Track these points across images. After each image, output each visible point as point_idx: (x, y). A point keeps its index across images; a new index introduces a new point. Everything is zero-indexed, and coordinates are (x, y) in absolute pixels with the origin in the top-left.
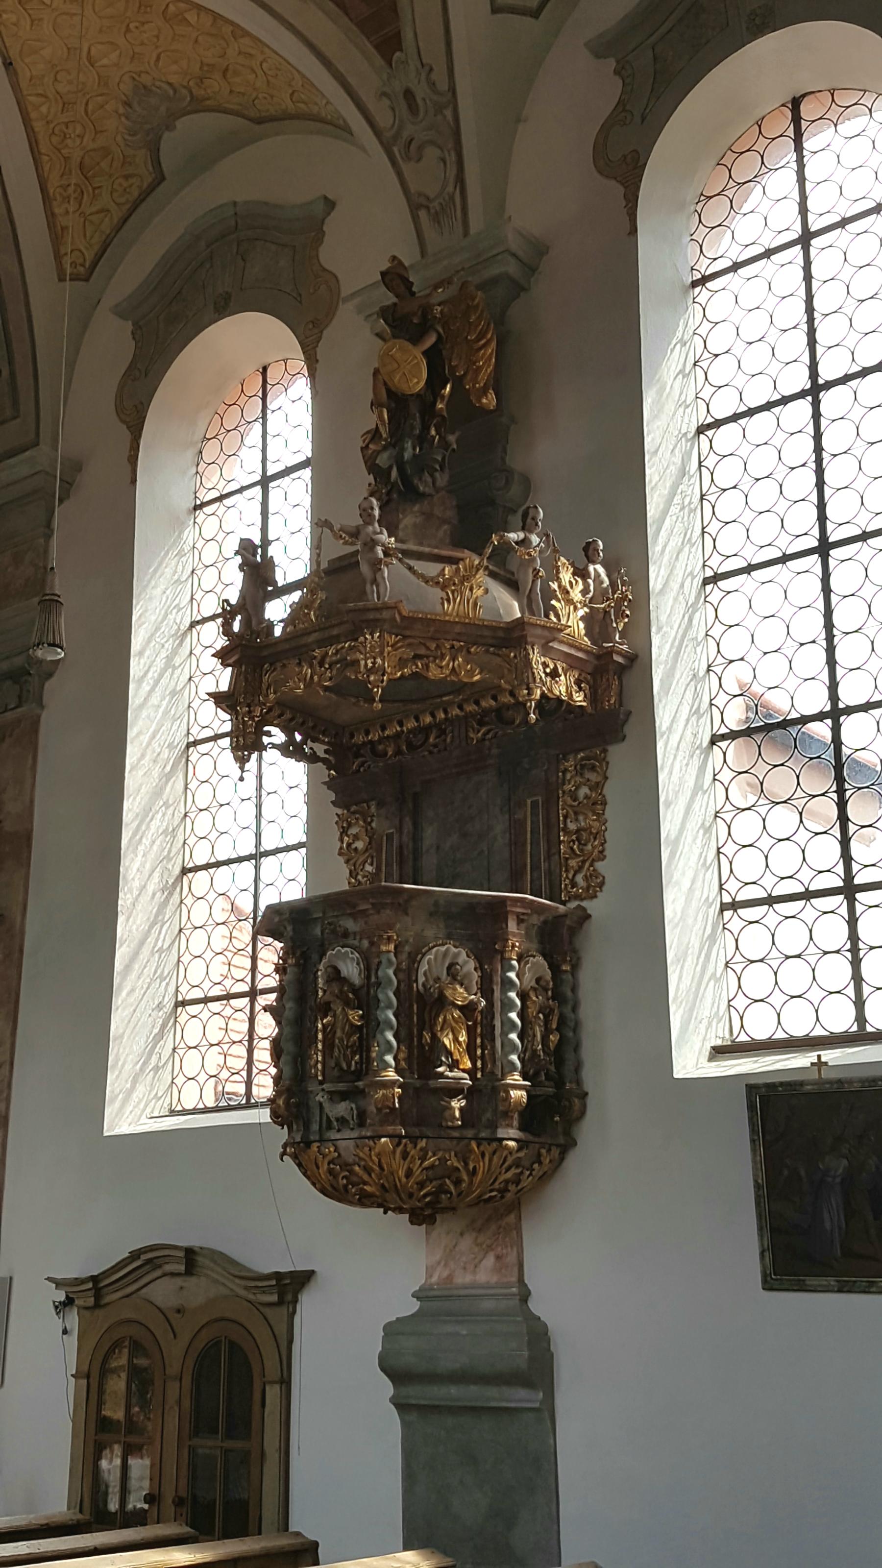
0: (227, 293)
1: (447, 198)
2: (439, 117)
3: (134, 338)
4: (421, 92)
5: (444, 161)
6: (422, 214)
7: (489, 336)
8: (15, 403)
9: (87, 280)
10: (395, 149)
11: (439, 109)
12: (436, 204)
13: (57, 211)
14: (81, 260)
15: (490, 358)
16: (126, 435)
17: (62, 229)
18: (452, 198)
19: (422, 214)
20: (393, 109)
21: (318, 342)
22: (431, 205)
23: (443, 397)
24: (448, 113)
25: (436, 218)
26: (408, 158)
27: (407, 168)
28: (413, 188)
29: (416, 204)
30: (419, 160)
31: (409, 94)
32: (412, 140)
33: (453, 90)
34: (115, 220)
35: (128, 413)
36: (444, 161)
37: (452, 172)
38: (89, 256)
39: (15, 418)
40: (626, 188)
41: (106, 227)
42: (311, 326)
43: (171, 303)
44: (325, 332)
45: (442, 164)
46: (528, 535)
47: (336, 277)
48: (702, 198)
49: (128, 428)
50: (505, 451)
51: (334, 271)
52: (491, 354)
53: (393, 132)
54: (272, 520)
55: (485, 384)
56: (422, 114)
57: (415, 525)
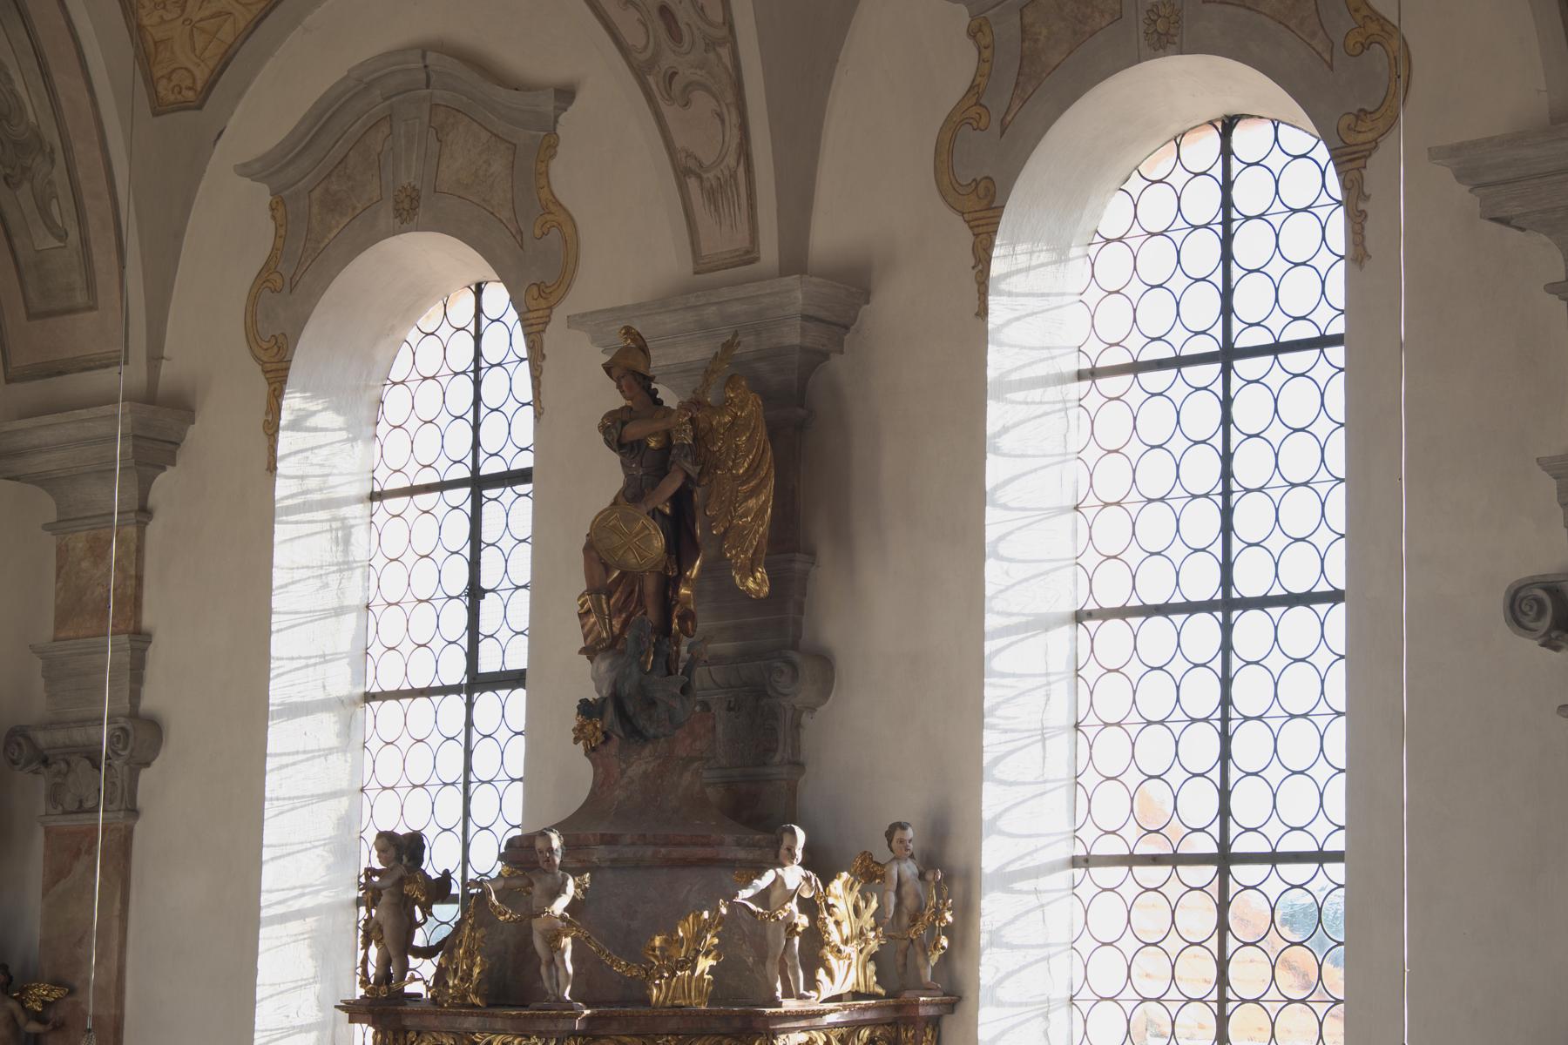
0: (414, 188)
1: (727, 172)
2: (712, 55)
3: (274, 217)
4: (684, 14)
6: (693, 183)
7: (763, 474)
8: (90, 286)
9: (200, 107)
10: (651, 79)
11: (712, 45)
12: (711, 175)
13: (146, 21)
14: (188, 82)
15: (762, 510)
16: (262, 386)
17: (155, 43)
18: (734, 176)
19: (693, 183)
20: (645, 25)
21: (547, 323)
22: (705, 176)
23: (687, 580)
24: (725, 52)
25: (712, 195)
27: (669, 111)
28: (680, 142)
30: (686, 104)
31: (665, 11)
32: (675, 74)
33: (729, 24)
34: (242, 25)
35: (265, 346)
38: (201, 74)
39: (91, 309)
40: (976, 235)
41: (227, 33)
42: (535, 289)
43: (329, 175)
44: (555, 310)
45: (717, 121)
46: (779, 870)
47: (572, 219)
48: (1097, 238)
49: (265, 372)
50: (801, 610)
51: (574, 215)
54: (487, 556)
56: (687, 38)
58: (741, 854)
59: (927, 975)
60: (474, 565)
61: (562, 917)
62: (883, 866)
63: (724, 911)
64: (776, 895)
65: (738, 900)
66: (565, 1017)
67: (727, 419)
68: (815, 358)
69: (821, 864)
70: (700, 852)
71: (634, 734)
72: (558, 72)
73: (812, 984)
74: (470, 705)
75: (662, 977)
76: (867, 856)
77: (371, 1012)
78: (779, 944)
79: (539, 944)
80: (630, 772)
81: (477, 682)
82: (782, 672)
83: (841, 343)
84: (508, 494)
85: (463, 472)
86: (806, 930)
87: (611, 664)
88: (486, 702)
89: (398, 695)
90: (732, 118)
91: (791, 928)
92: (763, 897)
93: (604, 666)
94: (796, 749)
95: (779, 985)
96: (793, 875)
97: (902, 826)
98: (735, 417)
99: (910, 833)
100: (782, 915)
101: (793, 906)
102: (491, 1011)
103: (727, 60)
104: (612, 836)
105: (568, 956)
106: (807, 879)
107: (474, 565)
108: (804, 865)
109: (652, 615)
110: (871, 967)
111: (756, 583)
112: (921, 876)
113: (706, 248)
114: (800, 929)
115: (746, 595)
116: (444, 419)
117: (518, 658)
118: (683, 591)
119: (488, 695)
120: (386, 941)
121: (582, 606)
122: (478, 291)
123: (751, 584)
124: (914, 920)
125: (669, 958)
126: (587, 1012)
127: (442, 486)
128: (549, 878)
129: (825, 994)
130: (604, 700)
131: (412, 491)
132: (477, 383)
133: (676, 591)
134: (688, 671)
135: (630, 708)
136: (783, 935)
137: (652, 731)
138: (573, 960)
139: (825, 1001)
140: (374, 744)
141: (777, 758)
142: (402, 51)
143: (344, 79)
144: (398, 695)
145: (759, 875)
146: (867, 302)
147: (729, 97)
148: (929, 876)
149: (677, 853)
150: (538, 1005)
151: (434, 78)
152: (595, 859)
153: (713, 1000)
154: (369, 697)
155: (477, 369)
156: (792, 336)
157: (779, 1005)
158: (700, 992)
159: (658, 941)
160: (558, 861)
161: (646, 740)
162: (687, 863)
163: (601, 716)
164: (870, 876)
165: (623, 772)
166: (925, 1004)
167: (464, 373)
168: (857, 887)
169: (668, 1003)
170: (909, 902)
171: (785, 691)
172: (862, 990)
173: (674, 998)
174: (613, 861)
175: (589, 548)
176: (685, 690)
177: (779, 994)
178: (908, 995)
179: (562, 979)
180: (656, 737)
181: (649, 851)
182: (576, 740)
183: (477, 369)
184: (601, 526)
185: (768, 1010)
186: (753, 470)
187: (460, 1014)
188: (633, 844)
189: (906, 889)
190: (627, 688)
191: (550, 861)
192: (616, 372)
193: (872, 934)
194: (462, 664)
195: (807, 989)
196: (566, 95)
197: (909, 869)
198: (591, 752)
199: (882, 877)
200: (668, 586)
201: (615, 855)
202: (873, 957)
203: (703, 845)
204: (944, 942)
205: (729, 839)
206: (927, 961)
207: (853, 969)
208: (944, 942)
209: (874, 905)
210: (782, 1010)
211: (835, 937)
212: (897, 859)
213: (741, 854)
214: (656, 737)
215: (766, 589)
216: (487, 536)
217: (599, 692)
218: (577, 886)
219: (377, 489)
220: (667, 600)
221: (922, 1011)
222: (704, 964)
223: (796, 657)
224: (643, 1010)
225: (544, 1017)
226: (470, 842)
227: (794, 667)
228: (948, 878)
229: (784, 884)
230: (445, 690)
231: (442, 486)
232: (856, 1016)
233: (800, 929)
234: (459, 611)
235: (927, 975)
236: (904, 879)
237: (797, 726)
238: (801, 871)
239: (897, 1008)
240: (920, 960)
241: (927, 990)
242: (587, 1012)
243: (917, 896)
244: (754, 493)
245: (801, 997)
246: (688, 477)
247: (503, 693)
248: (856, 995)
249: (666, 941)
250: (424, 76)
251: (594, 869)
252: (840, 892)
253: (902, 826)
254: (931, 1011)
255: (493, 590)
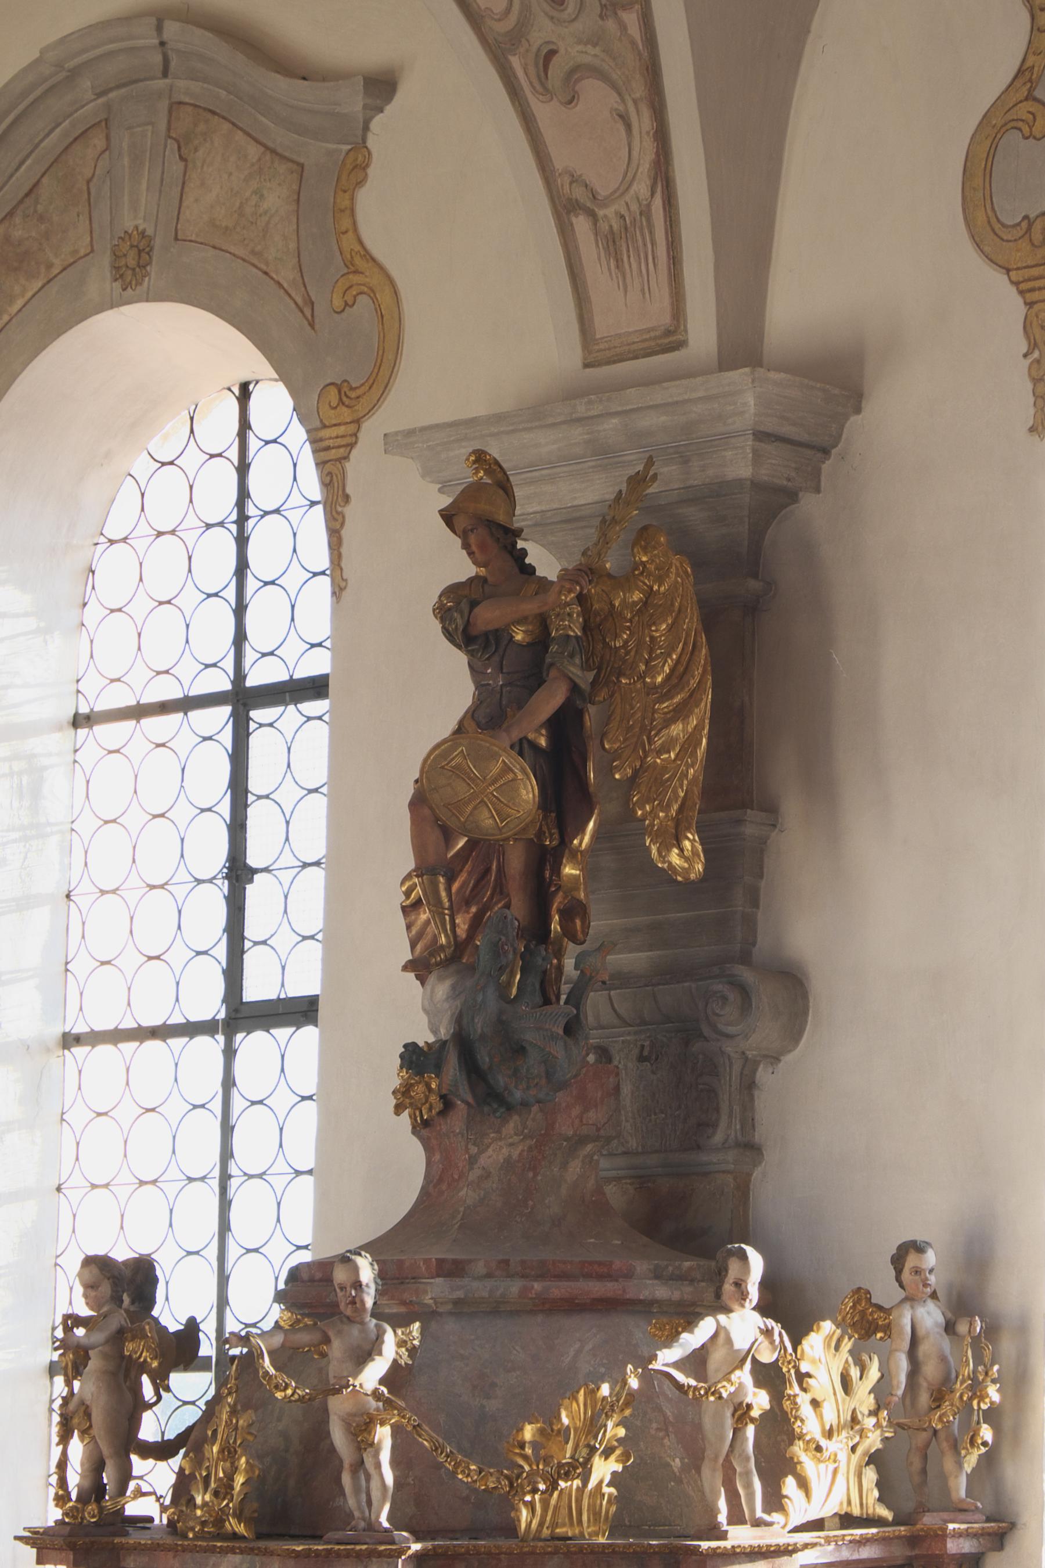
1: (634, 207)
2: (611, 24)
5: (624, 118)
6: (581, 224)
7: (693, 683)
10: (515, 61)
12: (610, 212)
18: (646, 212)
19: (581, 224)
22: (601, 213)
23: (574, 854)
25: (612, 244)
26: (546, 93)
27: (543, 111)
28: (560, 160)
29: (568, 204)
30: (571, 100)
32: (552, 53)
36: (624, 118)
37: (645, 152)
52: (698, 728)
53: (513, 18)
55: (680, 810)
57: (508, 1164)
58: (661, 1292)
59: (960, 1488)
60: (237, 828)
61: (376, 1394)
62: (887, 1311)
63: (634, 1383)
64: (717, 1357)
65: (655, 1366)
66: (380, 1555)
67: (637, 596)
68: (775, 500)
69: (789, 1307)
70: (597, 1289)
71: (491, 1100)
72: (368, 52)
73: (775, 1501)
74: (230, 1053)
75: (535, 1491)
76: (861, 1295)
77: (72, 1547)
78: (721, 1438)
79: (338, 1437)
80: (484, 1160)
81: (242, 1016)
82: (725, 998)
83: (817, 474)
84: (289, 716)
85: (222, 683)
86: (765, 1415)
87: (453, 987)
88: (256, 1046)
89: (116, 1036)
90: (643, 122)
91: (742, 1412)
92: (697, 1362)
93: (442, 989)
94: (749, 1122)
95: (722, 1504)
96: (745, 1326)
97: (917, 1247)
98: (650, 593)
99: (931, 1258)
100: (726, 1390)
101: (744, 1376)
102: (262, 1544)
103: (634, 30)
104: (455, 1262)
105: (385, 1456)
106: (768, 1333)
107: (237, 828)
108: (764, 1309)
109: (519, 908)
110: (870, 1475)
111: (686, 858)
112: (949, 1328)
113: (603, 326)
114: (755, 1413)
115: (667, 876)
116: (190, 598)
117: (305, 980)
118: (569, 870)
119: (259, 1035)
120: (95, 1431)
121: (408, 894)
122: (244, 393)
123: (674, 858)
124: (939, 1397)
125: (547, 1460)
126: (416, 1547)
127: (187, 704)
128: (355, 1331)
129: (796, 1520)
130: (443, 1044)
131: (139, 712)
132: (242, 541)
133: (557, 870)
134: (576, 998)
135: (484, 1058)
136: (729, 1422)
137: (518, 1095)
138: (394, 1463)
139: (797, 1530)
140: (78, 1116)
141: (718, 1138)
142: (127, 19)
143: (37, 62)
144: (116, 1036)
145: (690, 1322)
146: (858, 410)
147: (639, 89)
148: (962, 1328)
149: (559, 1289)
150: (339, 1535)
151: (173, 64)
152: (428, 1300)
153: (616, 1527)
154: (70, 1040)
155: (242, 519)
156: (739, 465)
157: (723, 1536)
158: (595, 1513)
159: (528, 1432)
160: (369, 1302)
161: (510, 1108)
162: (573, 1306)
163: (438, 1069)
164: (867, 1324)
165: (473, 1160)
166: (958, 1535)
167: (221, 524)
168: (847, 1345)
169: (546, 1532)
170: (931, 1370)
171: (731, 1030)
172: (856, 1511)
173: (554, 1525)
174: (457, 1302)
175: (419, 802)
176: (572, 1028)
177: (722, 1518)
178: (929, 1520)
179: (376, 1494)
180: (525, 1104)
181: (514, 1288)
182: (398, 1109)
183: (242, 519)
184: (437, 765)
185: (705, 1545)
186: (677, 678)
187: (213, 1550)
188: (489, 1276)
189: (923, 1349)
190: (479, 1025)
191: (356, 1303)
192: (461, 522)
193: (873, 1420)
194: (218, 987)
195: (768, 1509)
196: (382, 86)
197: (930, 1316)
198: (422, 1127)
199: (887, 1329)
200: (544, 860)
201: (460, 1294)
202: (874, 1459)
203: (601, 1277)
204: (987, 1433)
205: (642, 1267)
206: (960, 1465)
207: (841, 1479)
208: (987, 1433)
209: (874, 1373)
210: (727, 1544)
211: (811, 1425)
212: (910, 1299)
213: (661, 1292)
214: (525, 1104)
215: (699, 867)
216: (256, 783)
217: (434, 1031)
218: (401, 1344)
219: (84, 709)
220: (541, 886)
221: (953, 1546)
222: (603, 1469)
223: (746, 975)
224: (504, 1543)
225: (348, 1554)
226: (228, 1285)
227: (744, 991)
228: (992, 1331)
229: (729, 1341)
230: (191, 1029)
231: (187, 704)
232: (846, 1554)
233: (755, 1413)
234: (213, 904)
235: (960, 1488)
236: (921, 1332)
237: (749, 1086)
238: (757, 1320)
239: (913, 1541)
240: (949, 1464)
241: (959, 1510)
242: (416, 1547)
243: (943, 1359)
244: (680, 713)
245: (758, 1523)
246: (574, 688)
247: (282, 1033)
248: (846, 1520)
249: (541, 1432)
250: (158, 58)
251: (427, 1316)
252: (821, 1352)
253: (917, 1247)
254: (967, 1546)
255: (266, 870)
